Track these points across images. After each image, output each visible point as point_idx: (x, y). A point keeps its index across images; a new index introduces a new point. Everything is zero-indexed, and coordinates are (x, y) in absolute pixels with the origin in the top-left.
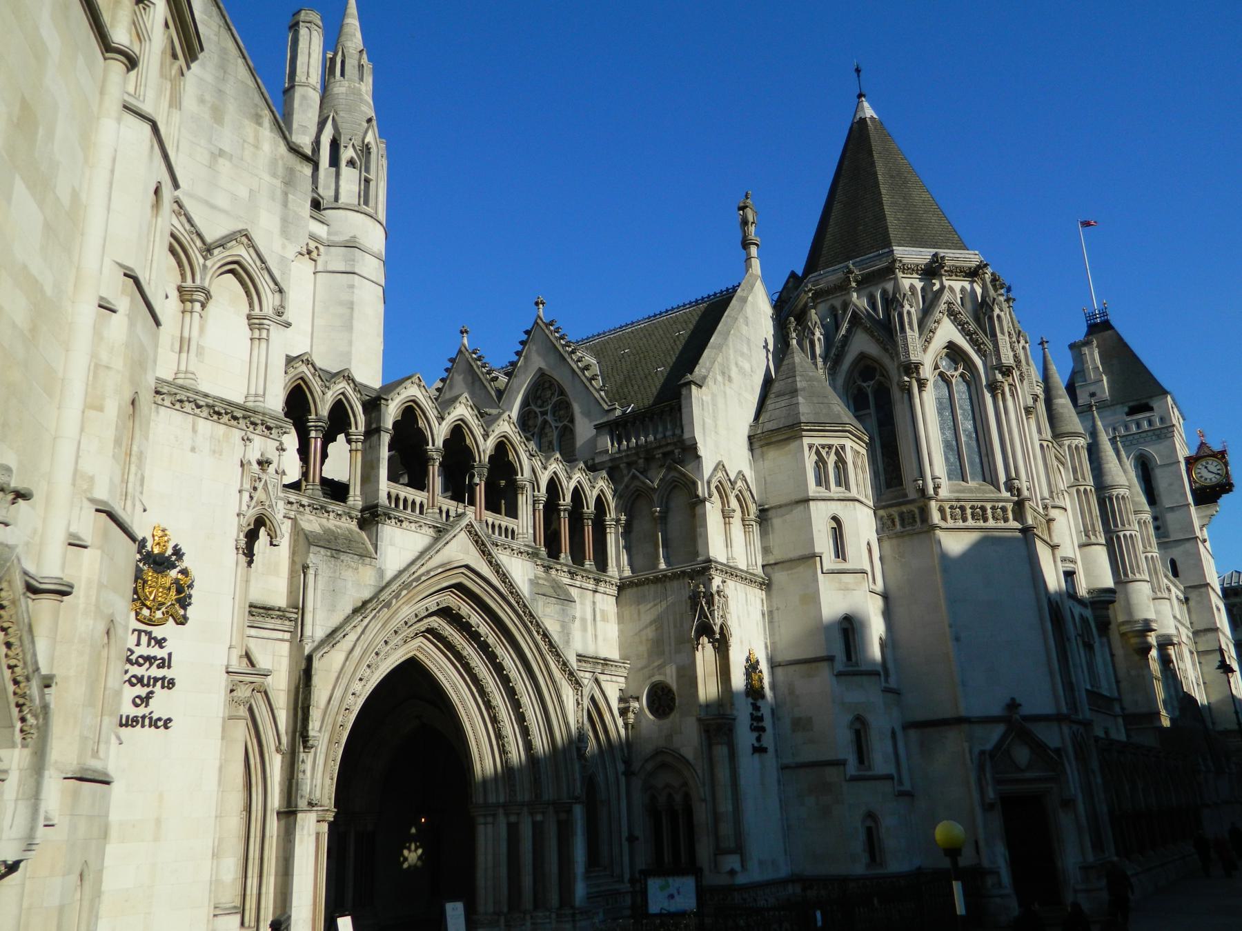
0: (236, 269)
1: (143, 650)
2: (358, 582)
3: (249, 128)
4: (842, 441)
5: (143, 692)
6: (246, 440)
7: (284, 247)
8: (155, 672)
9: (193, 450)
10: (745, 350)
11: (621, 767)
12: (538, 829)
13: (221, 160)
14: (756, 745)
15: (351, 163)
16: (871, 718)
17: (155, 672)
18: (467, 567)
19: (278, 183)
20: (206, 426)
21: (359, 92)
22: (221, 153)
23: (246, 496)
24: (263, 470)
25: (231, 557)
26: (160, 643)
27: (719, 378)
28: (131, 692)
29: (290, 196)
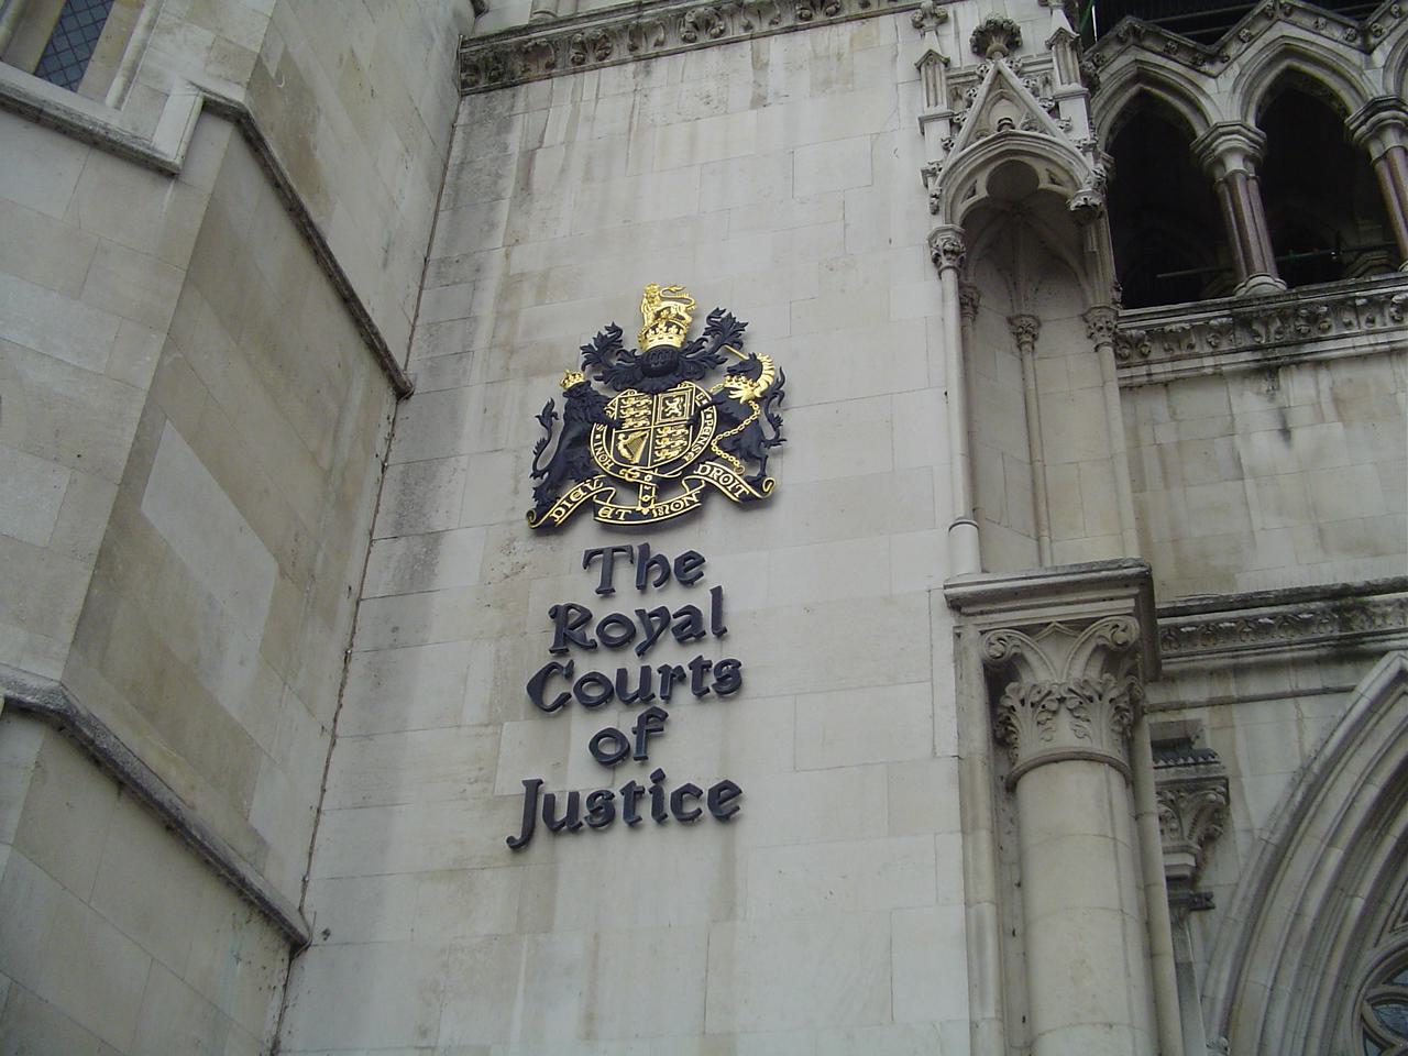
1: (627, 602)
5: (624, 720)
8: (670, 654)
9: (759, 101)
17: (670, 654)
23: (940, 130)
28: (582, 727)
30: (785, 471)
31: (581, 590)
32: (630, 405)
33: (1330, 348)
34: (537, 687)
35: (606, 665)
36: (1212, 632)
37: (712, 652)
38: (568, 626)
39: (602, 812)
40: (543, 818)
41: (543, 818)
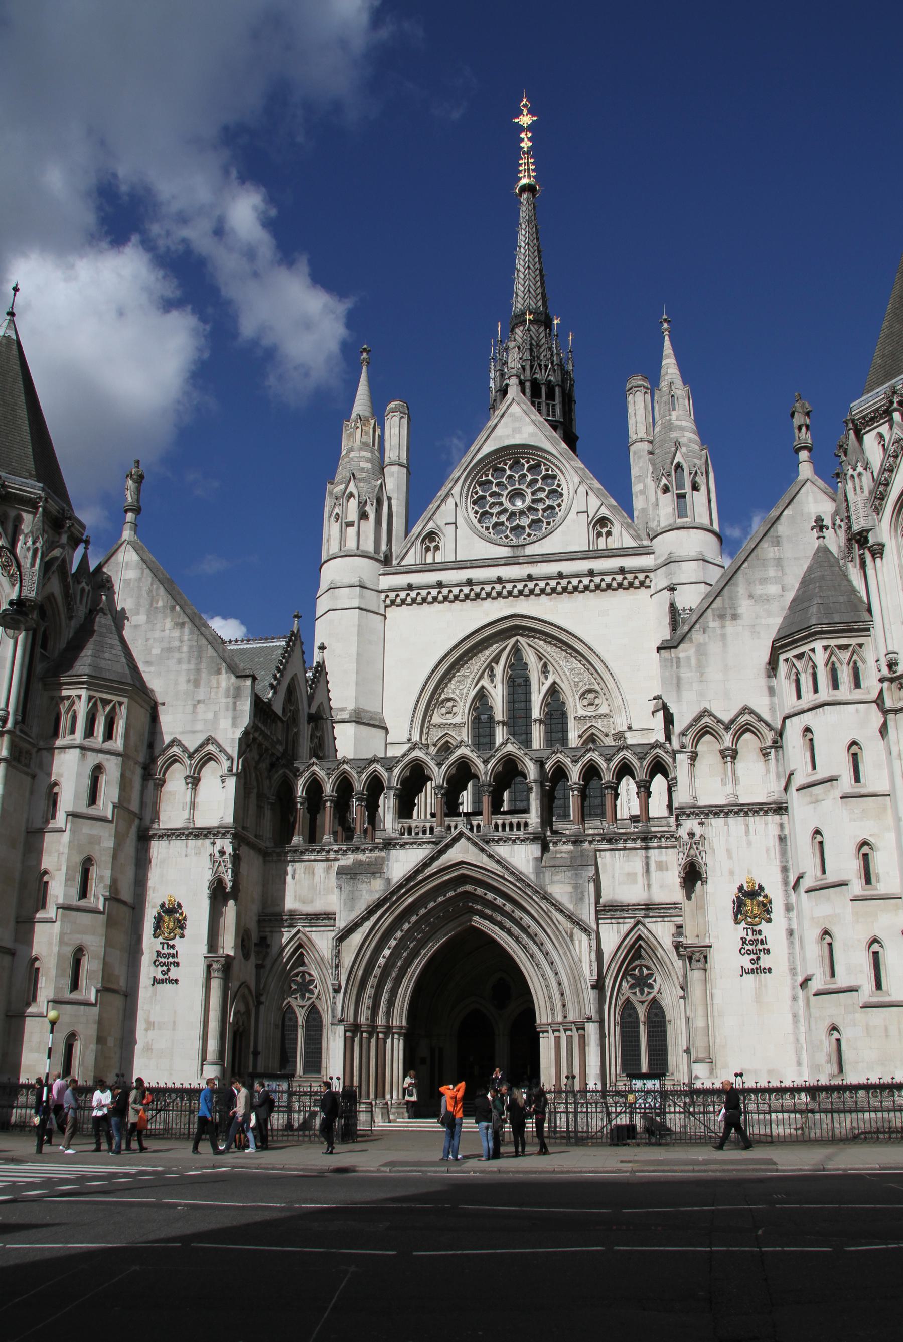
0: (210, 758)
1: (166, 951)
2: (372, 890)
3: (214, 679)
4: (812, 646)
6: (214, 843)
7: (234, 733)
8: (171, 960)
9: (186, 856)
10: (771, 572)
11: (681, 993)
12: (570, 1039)
13: (199, 706)
14: (751, 966)
15: (666, 490)
16: (834, 930)
17: (171, 960)
18: (462, 862)
19: (230, 700)
20: (192, 843)
21: (682, 419)
22: (199, 702)
24: (221, 856)
25: (205, 904)
26: (173, 947)
27: (713, 624)
28: (160, 969)
29: (238, 703)
30: (186, 932)
31: (159, 948)
32: (166, 918)
33: (305, 858)
34: (154, 962)
35: (163, 960)
36: (270, 920)
37: (175, 960)
38: (158, 953)
39: (162, 980)
40: (156, 981)
41: (156, 981)
